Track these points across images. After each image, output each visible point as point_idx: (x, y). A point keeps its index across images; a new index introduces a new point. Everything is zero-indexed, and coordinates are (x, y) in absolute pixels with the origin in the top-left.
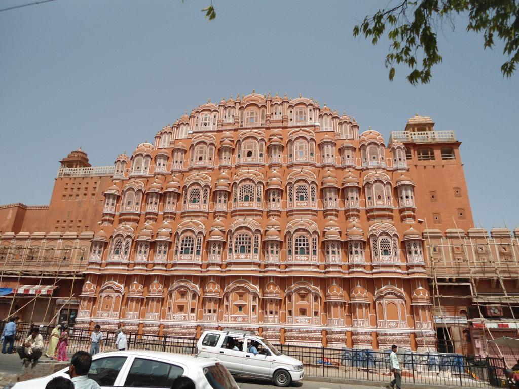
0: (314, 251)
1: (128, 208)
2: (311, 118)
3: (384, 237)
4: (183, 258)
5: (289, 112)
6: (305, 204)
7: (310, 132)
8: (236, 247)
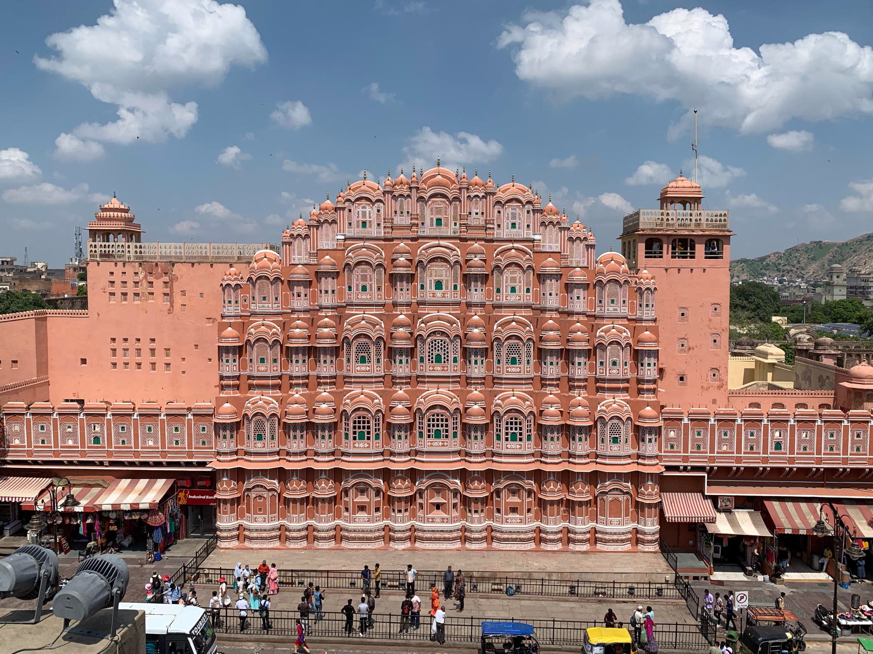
0: (529, 436)
1: (263, 369)
2: (528, 226)
3: (615, 421)
4: (357, 445)
5: (496, 211)
6: (518, 370)
7: (527, 253)
8: (429, 431)
